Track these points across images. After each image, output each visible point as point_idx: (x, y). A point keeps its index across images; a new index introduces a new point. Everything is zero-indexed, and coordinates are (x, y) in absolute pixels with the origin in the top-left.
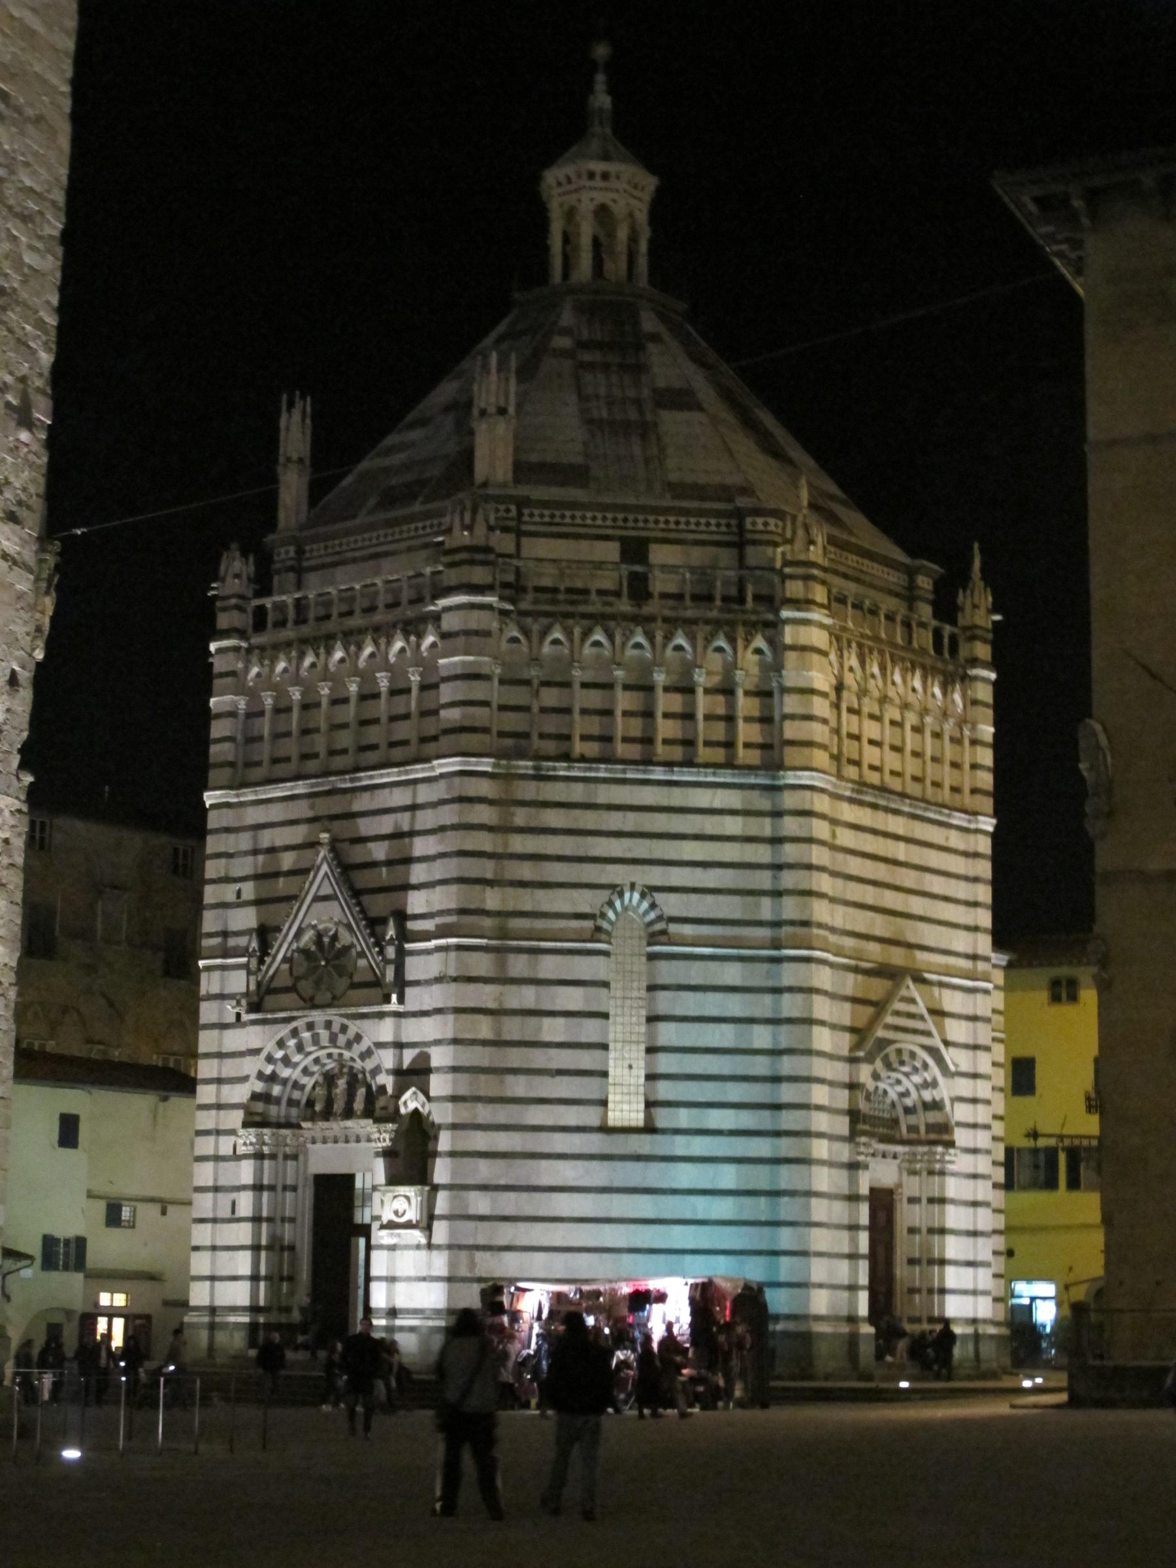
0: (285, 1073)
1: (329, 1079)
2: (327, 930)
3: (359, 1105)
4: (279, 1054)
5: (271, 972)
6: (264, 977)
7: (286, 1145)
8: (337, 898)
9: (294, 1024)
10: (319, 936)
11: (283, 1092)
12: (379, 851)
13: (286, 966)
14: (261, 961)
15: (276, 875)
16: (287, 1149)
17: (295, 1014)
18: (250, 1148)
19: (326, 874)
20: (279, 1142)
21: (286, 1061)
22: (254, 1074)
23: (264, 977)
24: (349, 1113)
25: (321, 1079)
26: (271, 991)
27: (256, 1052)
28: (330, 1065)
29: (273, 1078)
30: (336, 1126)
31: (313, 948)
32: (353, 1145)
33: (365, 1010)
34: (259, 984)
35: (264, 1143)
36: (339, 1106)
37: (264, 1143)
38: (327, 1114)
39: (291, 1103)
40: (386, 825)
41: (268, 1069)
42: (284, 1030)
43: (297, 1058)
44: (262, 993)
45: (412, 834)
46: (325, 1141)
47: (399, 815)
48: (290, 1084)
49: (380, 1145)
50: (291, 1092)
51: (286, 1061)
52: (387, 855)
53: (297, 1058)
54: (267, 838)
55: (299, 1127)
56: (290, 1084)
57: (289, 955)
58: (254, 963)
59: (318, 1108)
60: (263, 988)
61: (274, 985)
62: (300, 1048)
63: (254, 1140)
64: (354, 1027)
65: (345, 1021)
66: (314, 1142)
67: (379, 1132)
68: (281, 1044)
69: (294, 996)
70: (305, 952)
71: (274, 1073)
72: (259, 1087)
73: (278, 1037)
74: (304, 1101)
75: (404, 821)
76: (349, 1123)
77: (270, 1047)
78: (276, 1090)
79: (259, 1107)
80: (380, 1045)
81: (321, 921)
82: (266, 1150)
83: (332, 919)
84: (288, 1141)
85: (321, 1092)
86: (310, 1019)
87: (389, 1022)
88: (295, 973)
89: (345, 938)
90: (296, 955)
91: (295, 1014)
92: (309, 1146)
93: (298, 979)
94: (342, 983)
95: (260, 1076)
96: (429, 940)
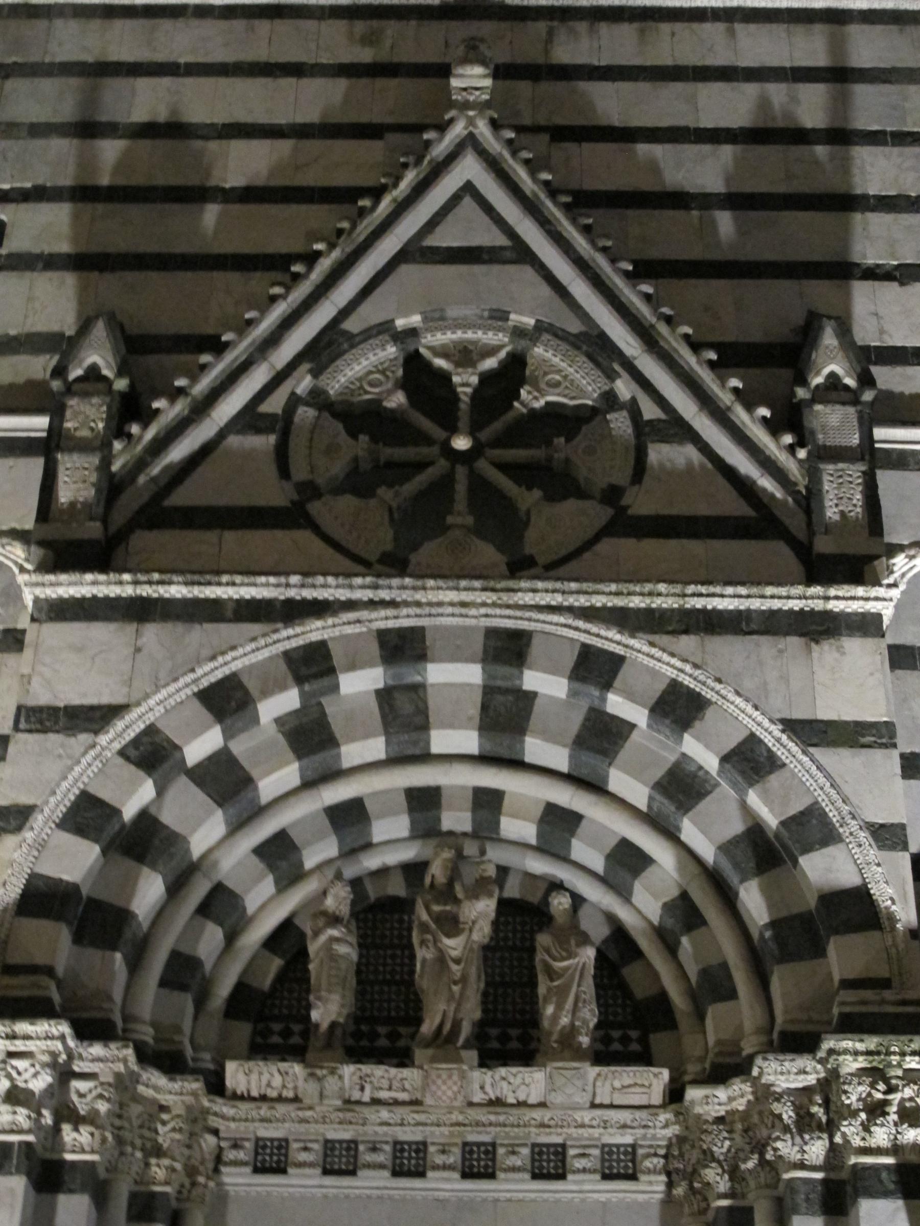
0: (204, 830)
1: (384, 917)
2: (465, 355)
3: (571, 1004)
4: (201, 746)
5: (178, 452)
6: (141, 464)
7: (158, 1152)
8: (522, 254)
9: (315, 630)
10: (418, 374)
11: (161, 914)
12: (704, 171)
13: (267, 442)
14: (130, 409)
15: (196, 195)
16: (158, 1171)
17: (328, 589)
18: (22, 1116)
19: (469, 188)
20: (130, 1122)
21: (225, 780)
22: (57, 804)
23: (141, 464)
24: (511, 1035)
25: (338, 900)
26: (158, 514)
27: (92, 718)
28: (392, 839)
29: (142, 841)
30: (448, 1094)
31: (397, 400)
32: (514, 1186)
33: (727, 600)
34: (112, 487)
35: (67, 1114)
36: (452, 999)
37: (67, 1114)
38: (384, 1029)
39: (183, 972)
40: (729, 106)
41: (136, 796)
42: (252, 652)
43: (278, 778)
44: (121, 515)
45: (841, 136)
46: (340, 1160)
47: (777, 92)
48: (199, 891)
49: (881, 1136)
50: (192, 932)
51: (225, 780)
52: (728, 180)
53: (278, 778)
54: (146, 101)
55: (216, 1086)
56: (199, 891)
57: (274, 404)
58: (87, 416)
59: (327, 1010)
60: (128, 504)
61: (181, 497)
62: (310, 737)
63: (40, 1082)
64: (655, 661)
65: (610, 639)
66: (272, 1160)
67: (875, 1074)
68: (227, 701)
69: (305, 536)
70: (358, 416)
71: (146, 820)
72: (76, 861)
73: (211, 673)
74: (224, 989)
75: (811, 107)
76: (526, 1083)
77: (164, 704)
78: (148, 892)
79: (54, 943)
80: (811, 733)
81: (436, 318)
82: (79, 1145)
83: (500, 315)
84: (166, 1135)
85: (335, 948)
86: (405, 620)
87: (861, 658)
88: (300, 472)
89: (563, 379)
90: (305, 414)
91: (328, 589)
92: (238, 1180)
93: (310, 490)
94: (555, 522)
95: (87, 815)
96: (604, 608)
